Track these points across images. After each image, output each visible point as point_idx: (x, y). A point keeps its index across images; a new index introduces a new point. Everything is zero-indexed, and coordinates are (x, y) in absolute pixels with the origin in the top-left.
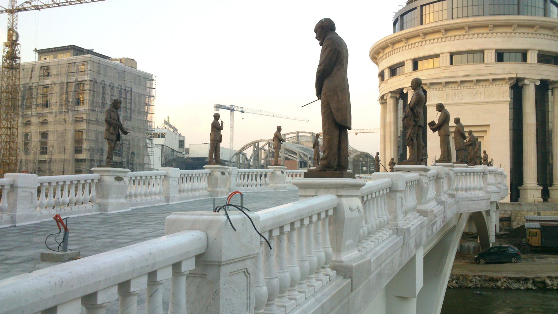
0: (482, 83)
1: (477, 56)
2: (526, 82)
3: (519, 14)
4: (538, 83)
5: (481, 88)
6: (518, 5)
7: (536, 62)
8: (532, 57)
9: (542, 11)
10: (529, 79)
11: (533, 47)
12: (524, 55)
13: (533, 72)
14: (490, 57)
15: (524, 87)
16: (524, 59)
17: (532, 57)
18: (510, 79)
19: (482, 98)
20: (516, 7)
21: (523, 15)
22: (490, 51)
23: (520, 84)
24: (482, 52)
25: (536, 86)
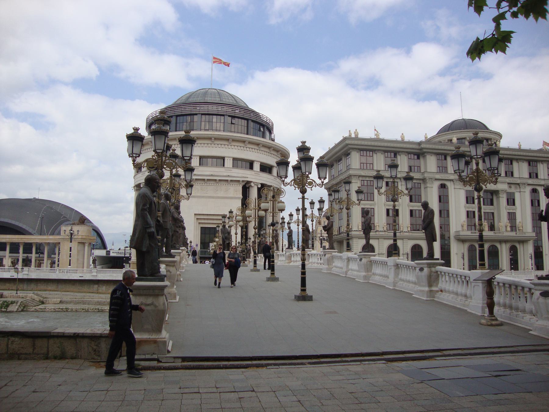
0: (222, 183)
1: (219, 160)
2: (252, 184)
3: (247, 134)
4: (260, 186)
5: (224, 186)
6: (247, 127)
7: (259, 170)
8: (257, 167)
9: (261, 133)
10: (254, 183)
11: (258, 160)
12: (251, 165)
13: (257, 177)
14: (229, 163)
15: (251, 188)
16: (251, 167)
17: (257, 167)
18: (243, 181)
19: (221, 194)
20: (246, 128)
21: (251, 135)
22: (229, 159)
23: (247, 186)
24: (223, 159)
25: (258, 188)
